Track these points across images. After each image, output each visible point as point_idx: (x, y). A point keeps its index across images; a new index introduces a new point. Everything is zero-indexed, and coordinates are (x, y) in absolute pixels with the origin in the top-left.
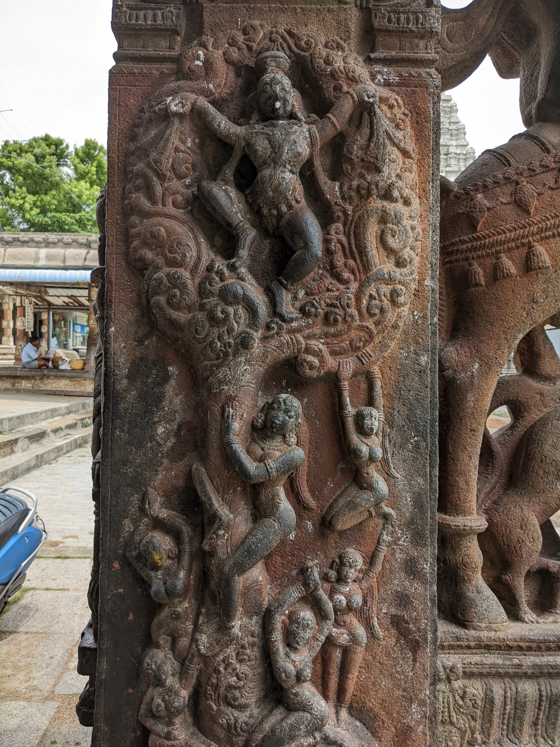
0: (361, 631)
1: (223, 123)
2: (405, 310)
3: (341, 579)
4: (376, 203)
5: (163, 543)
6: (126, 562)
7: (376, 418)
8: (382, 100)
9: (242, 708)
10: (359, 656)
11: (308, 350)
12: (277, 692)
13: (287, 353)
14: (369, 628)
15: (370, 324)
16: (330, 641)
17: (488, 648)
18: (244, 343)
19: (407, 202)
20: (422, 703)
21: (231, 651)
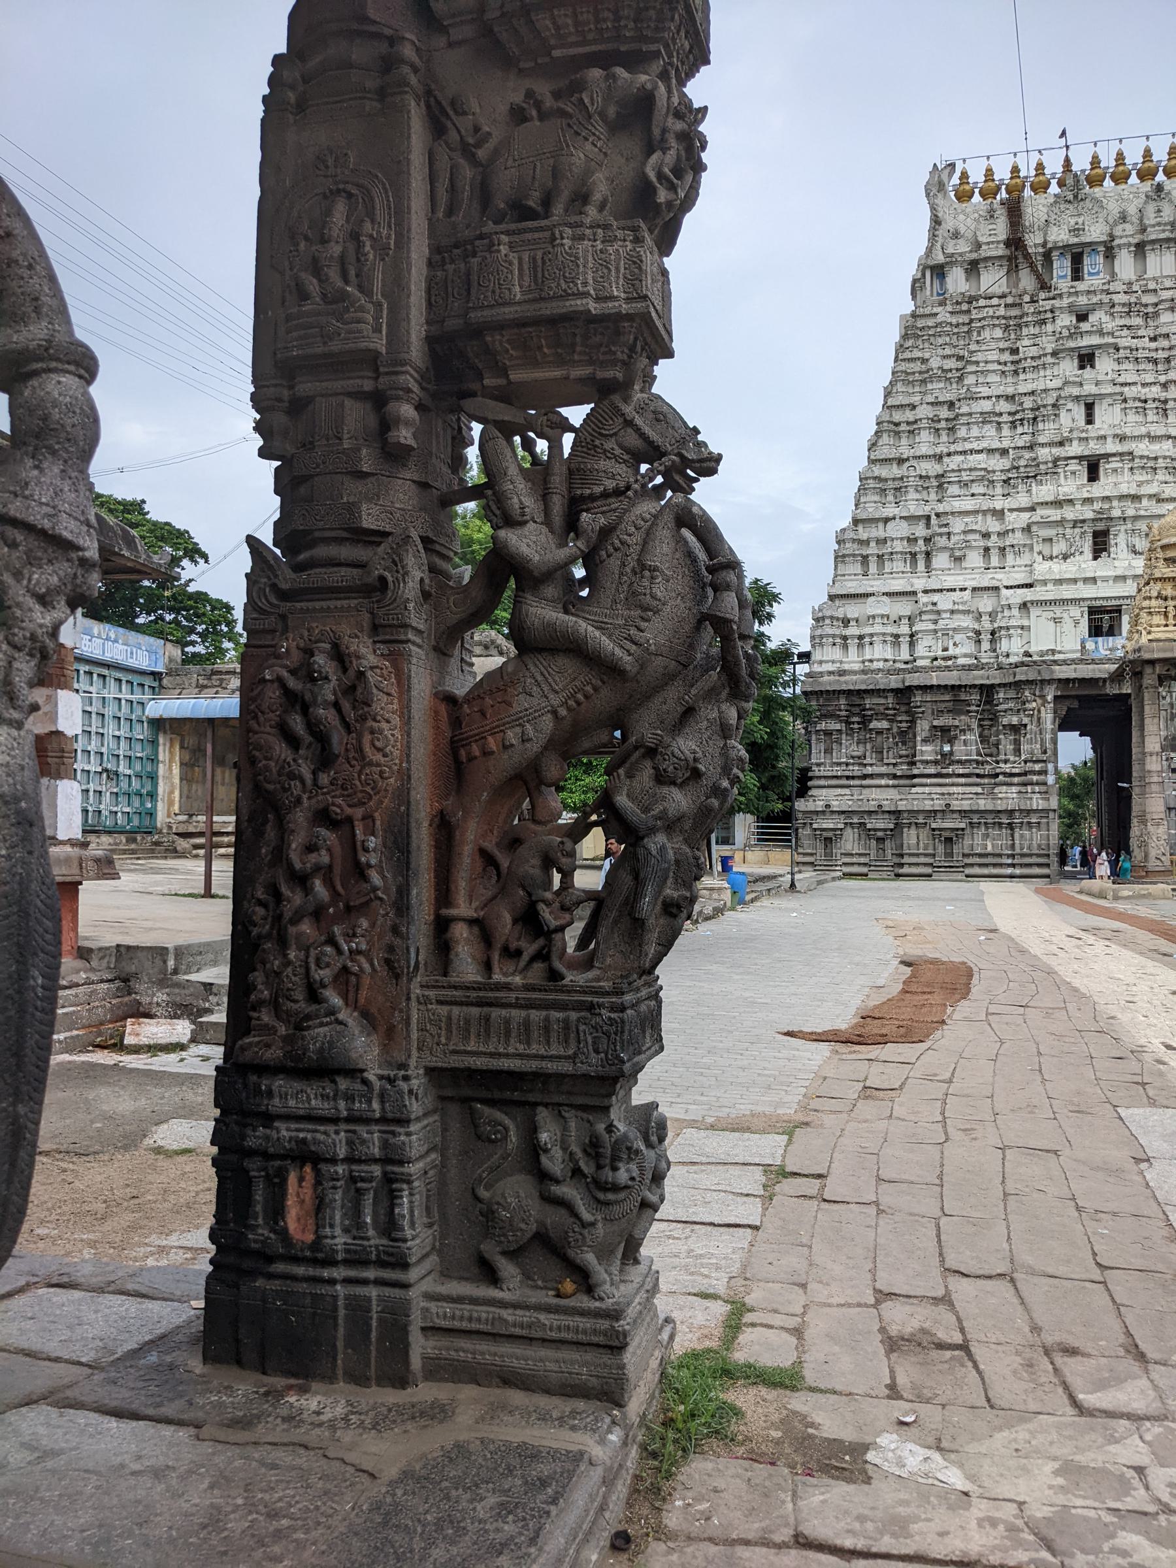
0: (366, 966)
1: (292, 683)
2: (392, 780)
3: (354, 935)
4: (370, 723)
5: (260, 911)
6: (244, 925)
7: (372, 842)
8: (372, 668)
9: (295, 1001)
10: (366, 981)
11: (333, 804)
12: (313, 995)
13: (321, 806)
14: (372, 965)
15: (368, 789)
16: (345, 969)
17: (455, 987)
18: (299, 801)
19: (388, 721)
20: (401, 1011)
21: (289, 969)
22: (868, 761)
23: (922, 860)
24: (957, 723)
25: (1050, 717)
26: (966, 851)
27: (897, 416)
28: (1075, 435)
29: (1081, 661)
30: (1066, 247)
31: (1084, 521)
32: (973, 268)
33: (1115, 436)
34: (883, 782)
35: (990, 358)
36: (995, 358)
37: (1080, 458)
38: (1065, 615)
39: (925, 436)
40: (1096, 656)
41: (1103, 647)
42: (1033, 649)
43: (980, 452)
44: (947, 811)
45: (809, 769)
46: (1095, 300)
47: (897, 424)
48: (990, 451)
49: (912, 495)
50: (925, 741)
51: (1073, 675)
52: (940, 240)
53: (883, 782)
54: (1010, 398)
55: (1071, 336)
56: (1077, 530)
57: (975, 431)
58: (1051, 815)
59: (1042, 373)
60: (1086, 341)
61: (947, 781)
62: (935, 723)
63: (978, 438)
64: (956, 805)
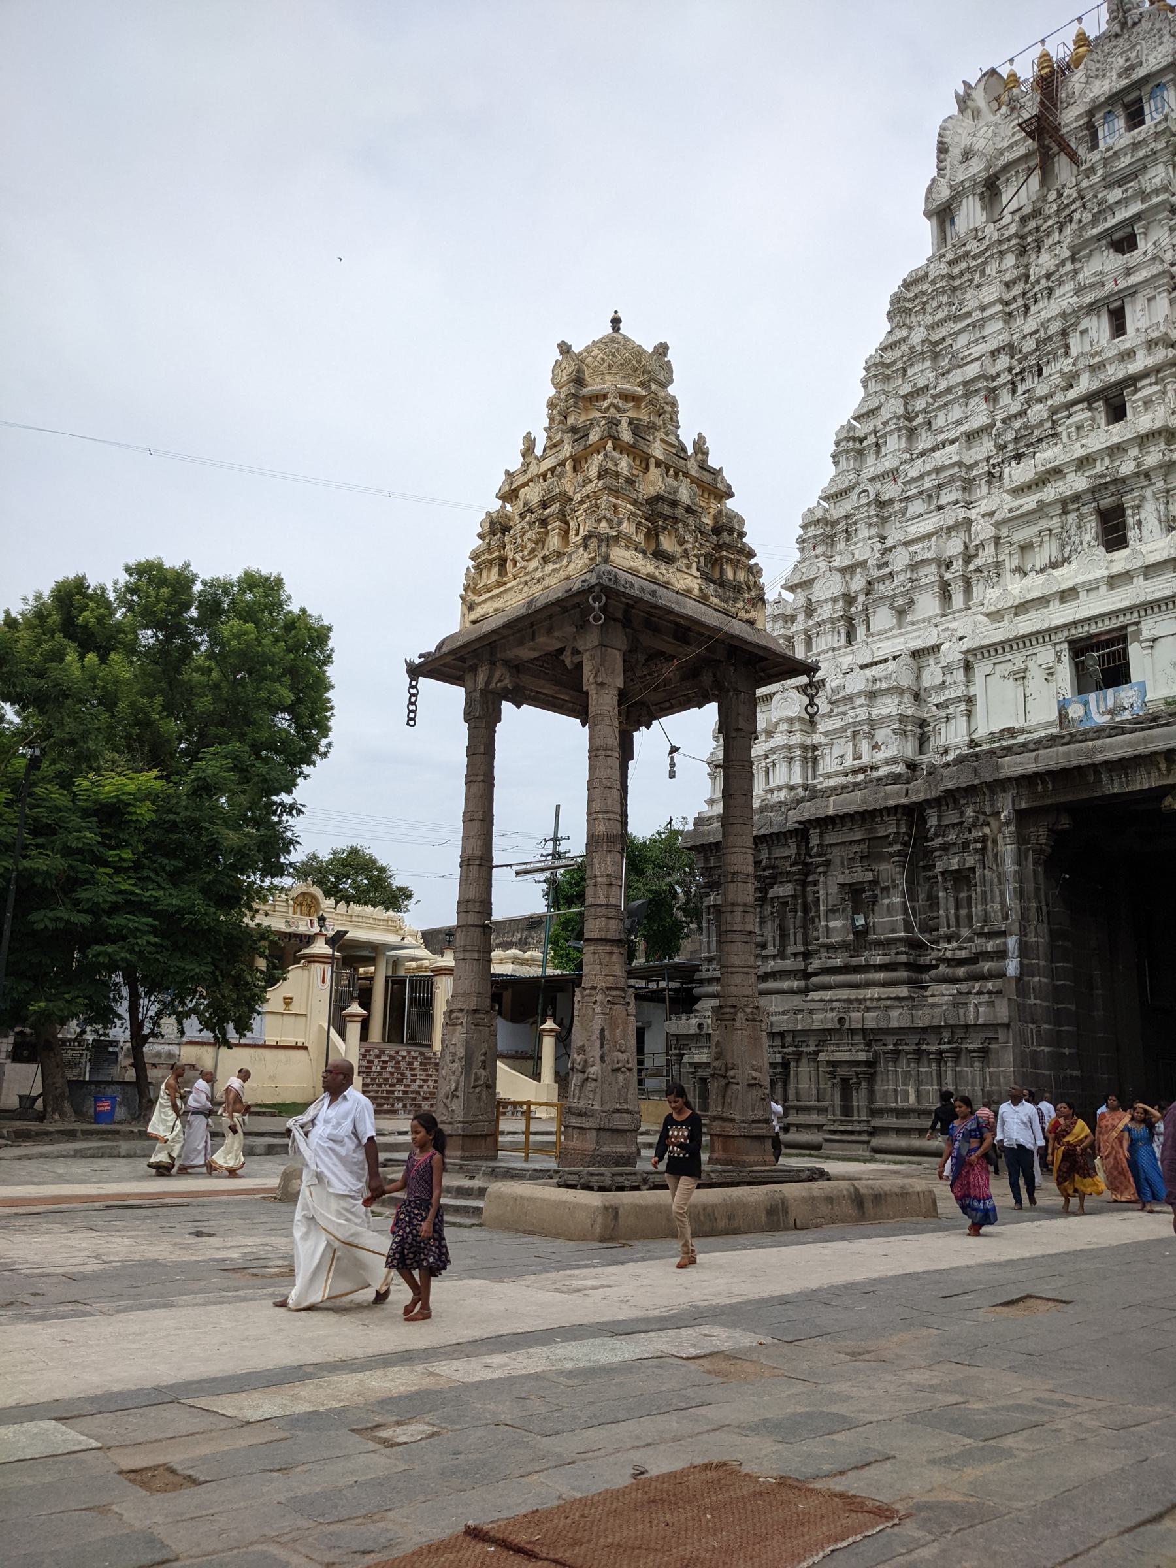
22: (771, 950)
23: (814, 1118)
24: (869, 876)
25: (1008, 851)
26: (879, 1104)
27: (861, 429)
28: (1081, 365)
29: (1053, 740)
30: (1114, 99)
31: (1076, 498)
32: (990, 189)
33: (1151, 345)
34: (785, 985)
35: (986, 300)
36: (994, 297)
37: (1089, 399)
38: (1031, 664)
39: (894, 443)
40: (1086, 726)
41: (1097, 709)
42: (981, 732)
43: (952, 442)
44: (841, 1032)
45: (697, 968)
46: (1141, 153)
47: (861, 441)
48: (971, 437)
49: (864, 532)
50: (832, 911)
51: (1033, 768)
52: (947, 172)
53: (785, 985)
54: (1010, 348)
55: (1094, 222)
56: (1072, 517)
57: (957, 412)
58: (1001, 1035)
59: (1058, 292)
60: (1122, 215)
61: (858, 978)
62: (841, 879)
63: (959, 422)
64: (855, 1018)
